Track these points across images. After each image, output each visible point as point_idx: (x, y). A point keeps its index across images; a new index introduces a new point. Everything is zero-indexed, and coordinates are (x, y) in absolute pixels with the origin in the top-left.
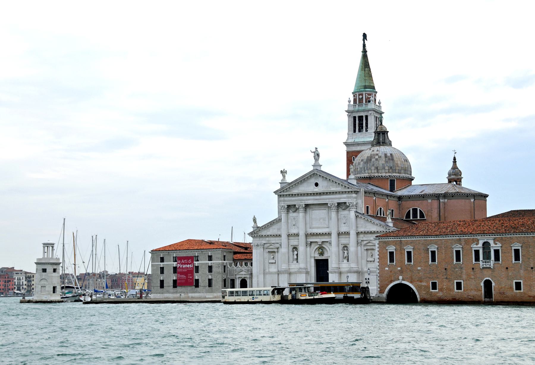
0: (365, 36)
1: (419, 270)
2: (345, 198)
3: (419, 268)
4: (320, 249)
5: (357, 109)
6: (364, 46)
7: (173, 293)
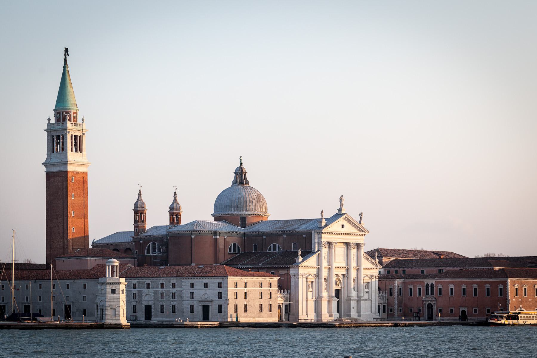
0: (67, 51)
1: (530, 301)
2: (359, 239)
3: (530, 300)
4: (339, 280)
5: (74, 128)
6: (66, 61)
7: (244, 317)
